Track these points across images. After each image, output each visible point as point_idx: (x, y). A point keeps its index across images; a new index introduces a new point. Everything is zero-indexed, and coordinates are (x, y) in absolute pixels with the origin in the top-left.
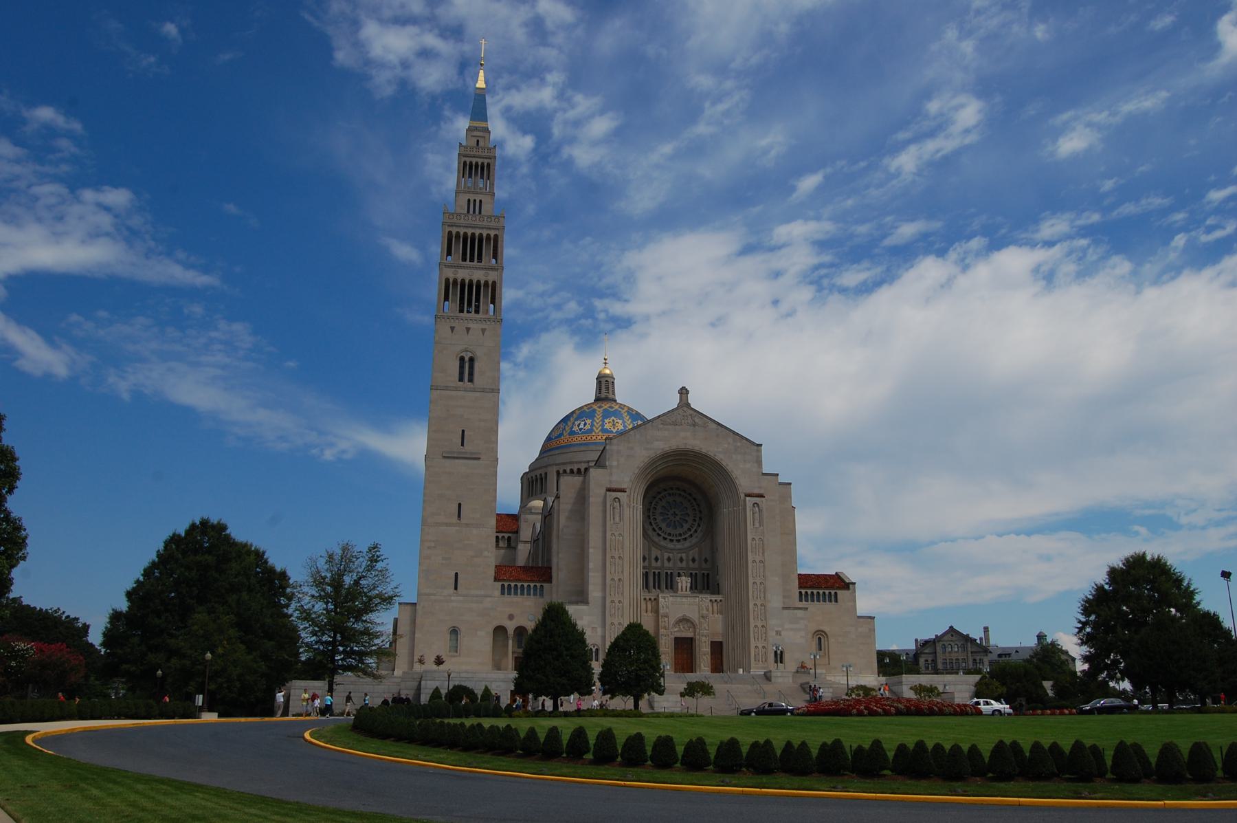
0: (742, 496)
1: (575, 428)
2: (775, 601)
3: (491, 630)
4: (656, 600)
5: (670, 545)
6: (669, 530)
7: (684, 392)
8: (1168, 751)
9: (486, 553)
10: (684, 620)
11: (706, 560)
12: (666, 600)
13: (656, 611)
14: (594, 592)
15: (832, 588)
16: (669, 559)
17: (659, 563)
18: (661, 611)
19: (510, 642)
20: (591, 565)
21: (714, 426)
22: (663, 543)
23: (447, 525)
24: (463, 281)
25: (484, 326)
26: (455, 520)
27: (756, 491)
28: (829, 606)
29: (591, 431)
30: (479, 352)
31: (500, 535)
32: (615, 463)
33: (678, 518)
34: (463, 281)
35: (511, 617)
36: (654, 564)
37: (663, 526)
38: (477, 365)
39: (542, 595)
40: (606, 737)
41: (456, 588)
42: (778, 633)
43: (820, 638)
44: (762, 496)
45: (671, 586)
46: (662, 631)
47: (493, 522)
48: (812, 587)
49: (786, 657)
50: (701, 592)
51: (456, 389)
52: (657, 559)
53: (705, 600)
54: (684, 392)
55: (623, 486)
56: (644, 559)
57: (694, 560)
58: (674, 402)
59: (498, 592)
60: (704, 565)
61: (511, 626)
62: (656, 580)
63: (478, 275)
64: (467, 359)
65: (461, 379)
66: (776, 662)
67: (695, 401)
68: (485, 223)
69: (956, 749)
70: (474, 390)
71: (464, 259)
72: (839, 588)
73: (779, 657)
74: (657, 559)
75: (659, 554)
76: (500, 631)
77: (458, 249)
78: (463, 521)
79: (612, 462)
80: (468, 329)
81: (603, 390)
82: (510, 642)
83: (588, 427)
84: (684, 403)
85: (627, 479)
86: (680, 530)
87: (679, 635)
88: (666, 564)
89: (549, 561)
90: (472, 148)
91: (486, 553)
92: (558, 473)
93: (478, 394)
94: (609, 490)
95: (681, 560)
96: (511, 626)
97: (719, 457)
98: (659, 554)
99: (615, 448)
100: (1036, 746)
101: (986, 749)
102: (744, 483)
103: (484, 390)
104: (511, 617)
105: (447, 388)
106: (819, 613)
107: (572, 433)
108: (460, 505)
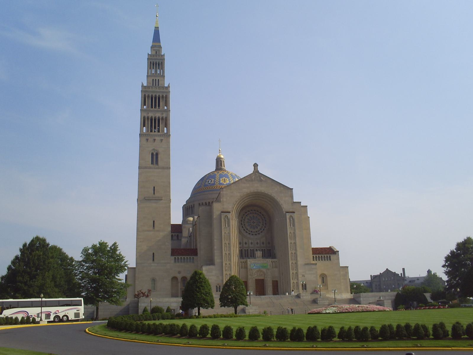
0: (284, 212)
1: (207, 183)
2: (301, 262)
3: (170, 278)
4: (246, 262)
7: (256, 165)
8: (456, 328)
11: (269, 243)
12: (250, 262)
13: (246, 268)
14: (217, 260)
15: (328, 253)
16: (252, 243)
17: (247, 246)
18: (249, 267)
19: (179, 284)
20: (215, 247)
22: (248, 236)
23: (148, 231)
24: (152, 117)
25: (162, 138)
26: (151, 228)
27: (291, 210)
28: (327, 262)
30: (160, 150)
31: (173, 234)
32: (225, 200)
33: (255, 224)
34: (152, 117)
35: (179, 272)
36: (245, 245)
37: (248, 228)
38: (159, 156)
39: (193, 262)
40: (215, 328)
41: (153, 260)
42: (303, 276)
43: (323, 277)
45: (253, 256)
46: (249, 277)
47: (170, 229)
48: (318, 254)
49: (308, 286)
50: (267, 258)
51: (150, 168)
52: (246, 243)
53: (268, 262)
54: (256, 165)
55: (229, 210)
56: (240, 243)
57: (263, 243)
58: (251, 170)
59: (173, 261)
61: (179, 276)
62: (245, 254)
63: (158, 115)
64: (155, 153)
65: (152, 163)
66: (303, 289)
67: (261, 170)
68: (161, 90)
69: (365, 329)
70: (159, 168)
71: (152, 107)
72: (331, 254)
73: (304, 287)
74: (246, 243)
76: (174, 278)
77: (148, 102)
78: (156, 228)
79: (224, 199)
80: (155, 140)
81: (219, 165)
82: (179, 284)
83: (213, 182)
84: (256, 171)
86: (257, 230)
87: (257, 278)
88: (250, 245)
89: (196, 245)
90: (154, 56)
92: (199, 204)
94: (223, 212)
95: (257, 243)
96: (179, 276)
97: (274, 195)
99: (224, 192)
100: (399, 326)
101: (378, 328)
102: (286, 207)
103: (163, 168)
104: (179, 272)
105: (146, 168)
106: (322, 266)
107: (205, 185)
108: (154, 221)
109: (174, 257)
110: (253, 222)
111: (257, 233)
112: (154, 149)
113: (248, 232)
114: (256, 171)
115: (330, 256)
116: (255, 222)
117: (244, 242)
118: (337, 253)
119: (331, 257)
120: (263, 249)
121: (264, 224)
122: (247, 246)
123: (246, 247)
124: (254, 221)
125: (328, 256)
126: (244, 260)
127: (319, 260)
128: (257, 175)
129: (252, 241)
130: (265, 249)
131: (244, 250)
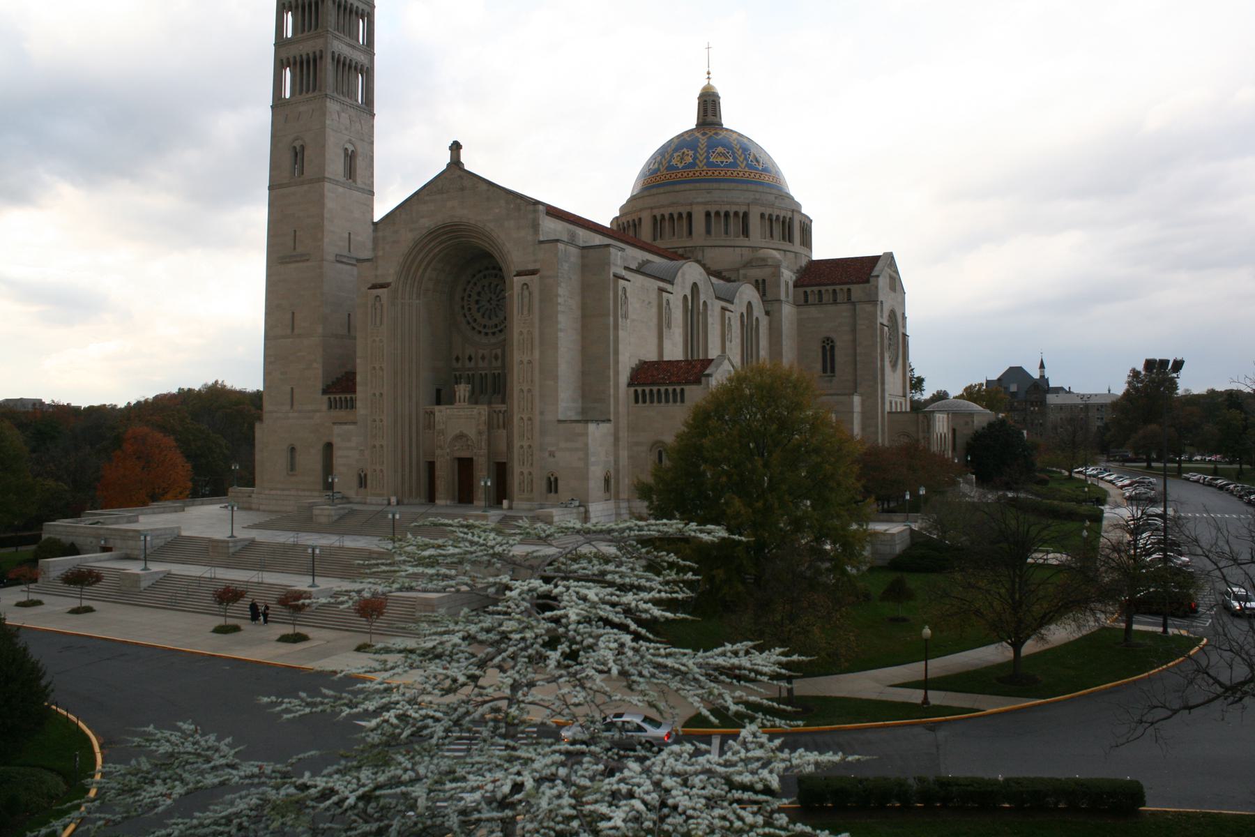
3: (320, 447)
7: (456, 147)
9: (315, 365)
10: (461, 436)
12: (442, 412)
15: (679, 383)
16: (483, 358)
17: (472, 364)
21: (485, 187)
29: (693, 165)
37: (478, 316)
41: (292, 405)
42: (552, 454)
44: (533, 272)
54: (456, 147)
59: (325, 407)
70: (302, 183)
72: (688, 383)
74: (470, 359)
78: (296, 331)
81: (710, 112)
84: (455, 163)
85: (392, 271)
88: (481, 364)
91: (315, 365)
92: (708, 214)
93: (306, 187)
94: (374, 287)
103: (311, 181)
109: (326, 397)
112: (296, 139)
114: (455, 163)
115: (682, 390)
118: (703, 379)
119: (686, 394)
123: (469, 369)
125: (678, 389)
127: (644, 402)
128: (455, 177)
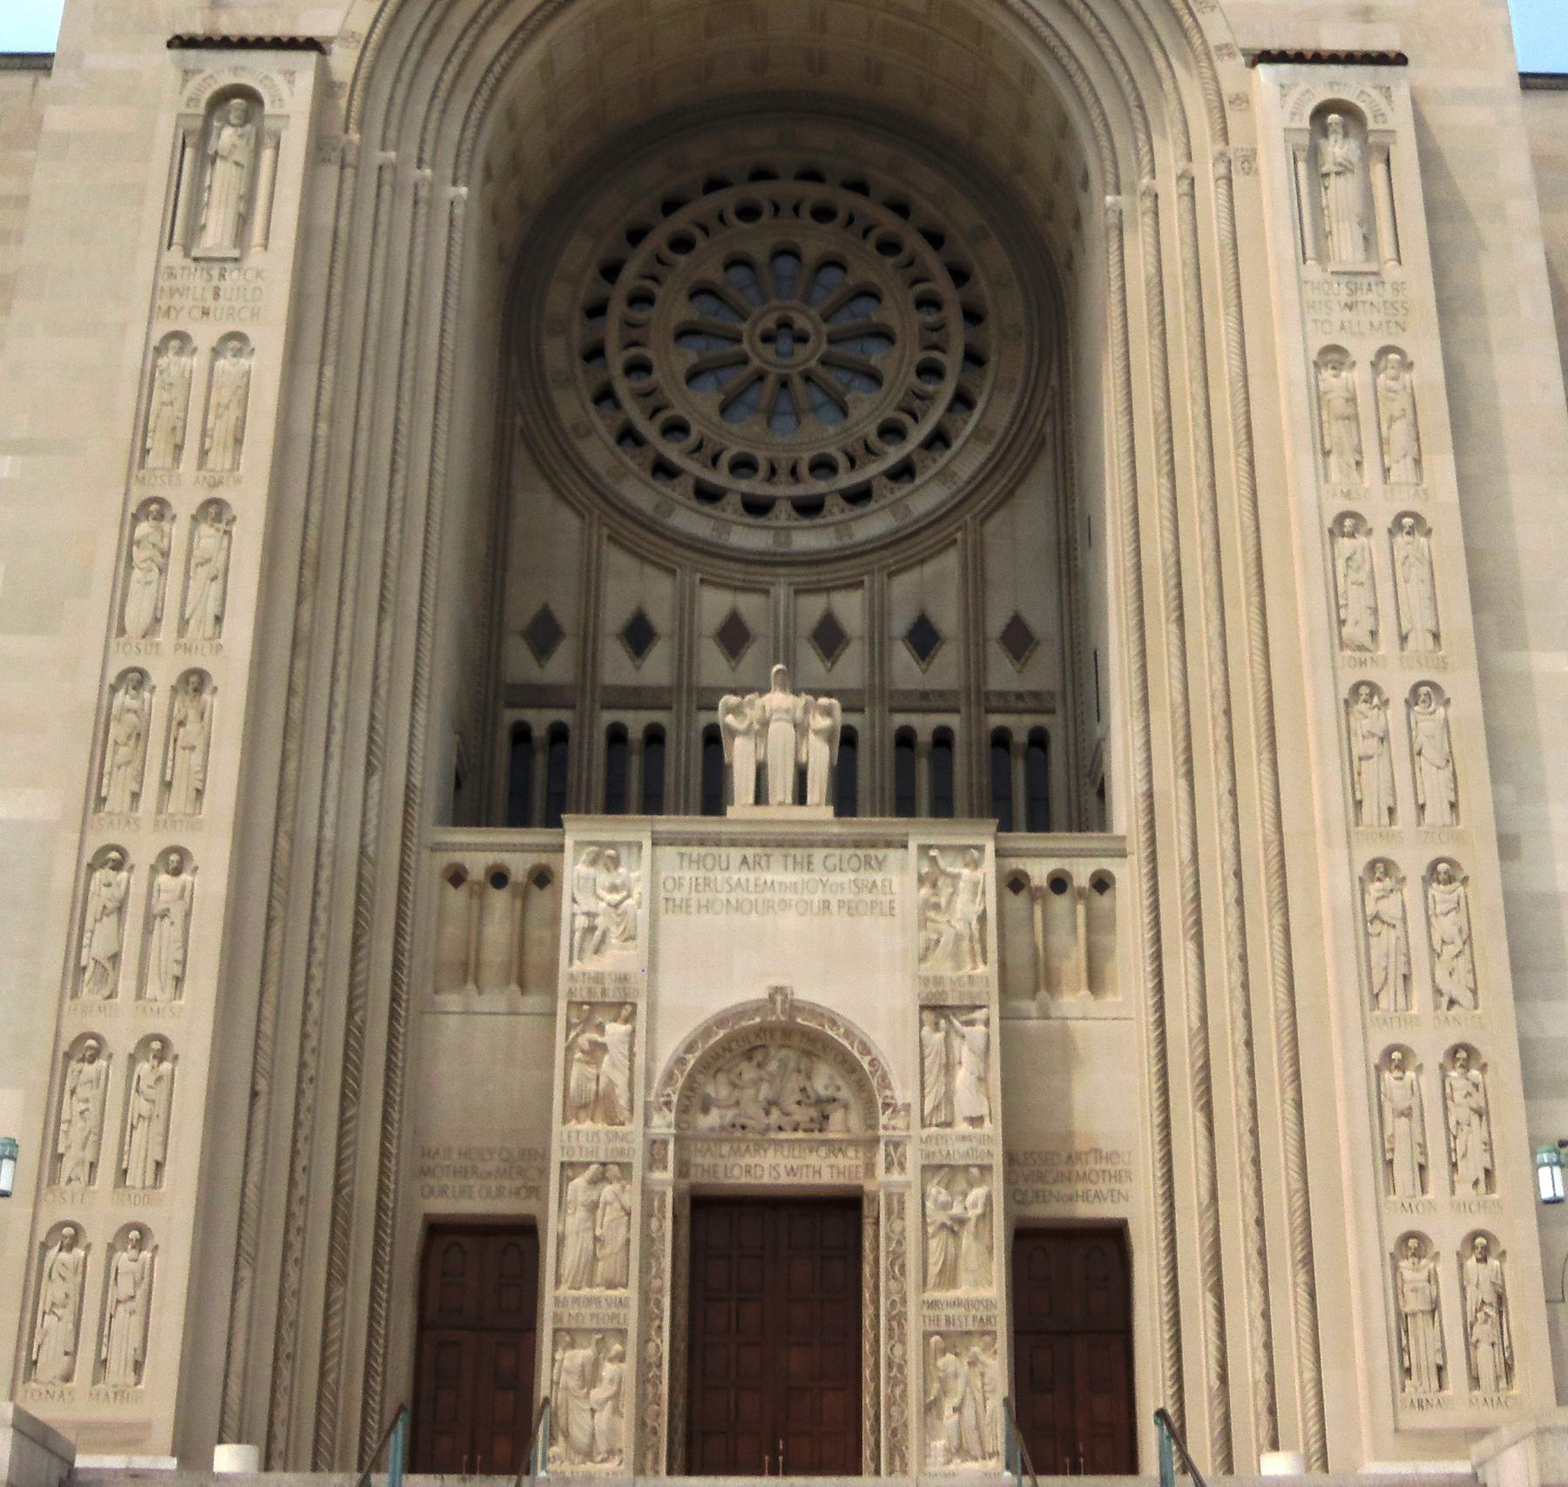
4: (543, 878)
5: (748, 537)
6: (740, 436)
10: (776, 1045)
11: (1018, 639)
22: (691, 521)
60: (1002, 675)
75: (656, 594)
98: (656, 594)
110: (785, 324)
111: (819, 486)
113: (694, 468)
116: (802, 339)
117: (615, 616)
120: (924, 725)
121: (952, 361)
122: (657, 668)
123: (635, 698)
124: (801, 322)
126: (513, 847)
129: (750, 606)
130: (953, 721)
131: (600, 739)
